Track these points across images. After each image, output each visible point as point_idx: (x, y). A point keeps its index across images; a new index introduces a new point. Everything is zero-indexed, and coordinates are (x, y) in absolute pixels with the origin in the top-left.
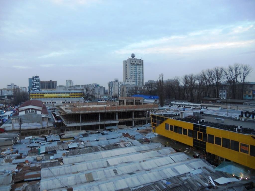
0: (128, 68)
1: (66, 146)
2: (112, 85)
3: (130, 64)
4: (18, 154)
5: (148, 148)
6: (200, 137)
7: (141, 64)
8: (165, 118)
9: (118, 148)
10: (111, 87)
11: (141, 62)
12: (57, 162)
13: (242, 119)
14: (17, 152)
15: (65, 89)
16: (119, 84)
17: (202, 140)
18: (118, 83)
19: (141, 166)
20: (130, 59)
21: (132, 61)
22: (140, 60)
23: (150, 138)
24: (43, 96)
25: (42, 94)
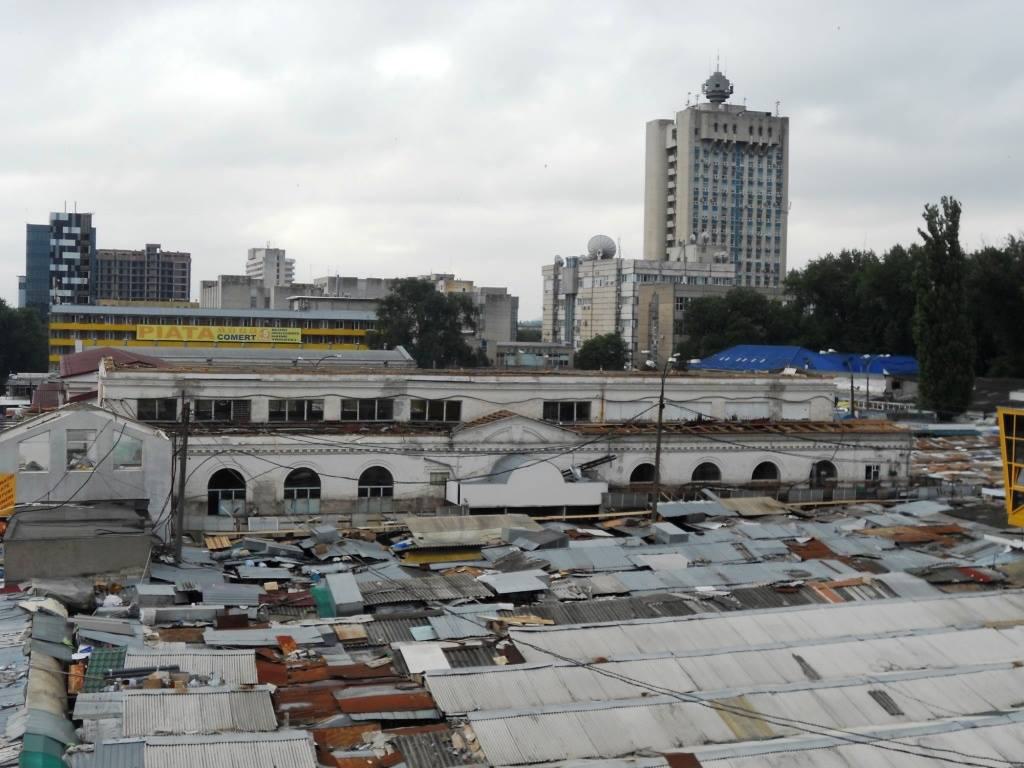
0: (683, 172)
1: (475, 584)
2: (577, 282)
3: (699, 145)
7: (774, 145)
9: (806, 602)
11: (770, 130)
12: (477, 648)
15: (260, 303)
16: (621, 277)
18: (619, 270)
20: (695, 113)
21: (713, 121)
22: (769, 114)
23: (992, 567)
24: (133, 334)
25: (126, 327)
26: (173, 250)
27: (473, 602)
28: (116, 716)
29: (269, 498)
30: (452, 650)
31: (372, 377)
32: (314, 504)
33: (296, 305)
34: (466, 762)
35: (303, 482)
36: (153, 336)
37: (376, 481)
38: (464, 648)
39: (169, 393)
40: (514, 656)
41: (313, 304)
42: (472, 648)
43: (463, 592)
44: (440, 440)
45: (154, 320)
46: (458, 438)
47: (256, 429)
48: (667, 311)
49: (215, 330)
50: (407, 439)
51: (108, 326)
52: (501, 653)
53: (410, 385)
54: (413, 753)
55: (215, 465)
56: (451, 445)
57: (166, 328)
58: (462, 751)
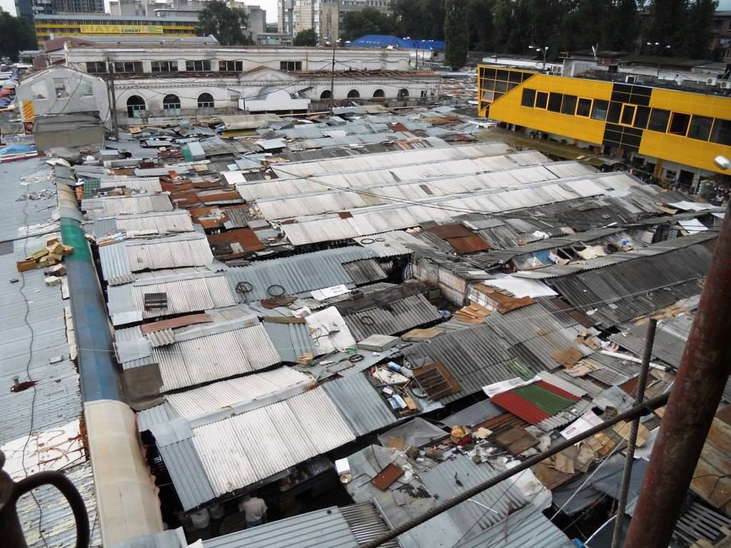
1: (254, 145)
5: (478, 153)
6: (627, 119)
8: (524, 74)
9: (396, 150)
10: (289, 10)
13: (724, 84)
15: (140, 12)
17: (632, 126)
19: (482, 181)
23: (471, 134)
24: (79, 30)
25: (75, 26)
28: (101, 208)
29: (157, 109)
30: (247, 174)
31: (199, 50)
32: (178, 111)
34: (256, 219)
37: (206, 99)
38: (251, 173)
39: (101, 59)
40: (273, 176)
41: (167, 13)
42: (255, 173)
45: (88, 22)
46: (242, 79)
47: (146, 76)
48: (335, 18)
49: (120, 27)
50: (219, 80)
51: (65, 26)
53: (218, 54)
55: (129, 93)
56: (239, 82)
58: (254, 215)
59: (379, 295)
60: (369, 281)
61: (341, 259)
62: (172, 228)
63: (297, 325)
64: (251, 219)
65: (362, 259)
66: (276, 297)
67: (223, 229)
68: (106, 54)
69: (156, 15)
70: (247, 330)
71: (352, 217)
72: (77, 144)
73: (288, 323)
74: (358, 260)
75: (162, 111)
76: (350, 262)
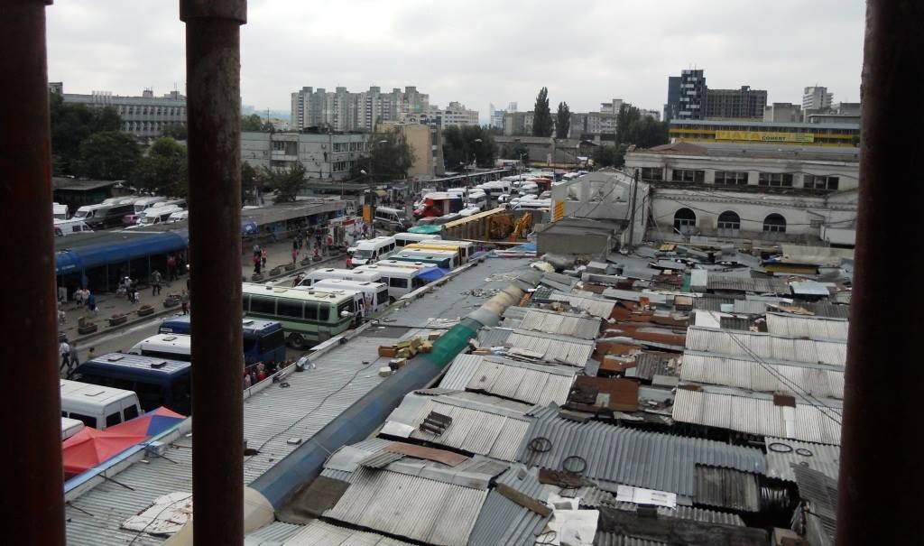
1: (784, 286)
4: (623, 278)
12: (743, 320)
14: (620, 272)
15: (797, 118)
24: (714, 135)
25: (710, 132)
26: (714, 89)
27: (775, 296)
28: (521, 318)
29: (709, 226)
30: (727, 318)
31: (779, 161)
32: (735, 232)
33: (812, 120)
34: (670, 375)
35: (730, 219)
36: (725, 137)
37: (775, 221)
38: (735, 319)
39: (659, 165)
40: (763, 327)
41: (822, 119)
42: (740, 320)
43: (773, 290)
44: (820, 200)
45: (726, 128)
46: (831, 200)
47: (704, 187)
49: (761, 134)
50: (797, 198)
51: (700, 131)
52: (756, 324)
53: (803, 166)
54: (643, 364)
55: (677, 206)
56: (826, 204)
57: (732, 133)
58: (671, 369)
59: (686, 526)
60: (721, 505)
61: (698, 456)
62: (563, 358)
63: (532, 514)
64: (663, 372)
65: (734, 469)
66: (569, 472)
67: (622, 374)
68: (665, 160)
69: (810, 121)
70: (467, 490)
71: (794, 406)
72: (576, 251)
73: (523, 507)
74: (726, 468)
75: (715, 230)
76: (712, 467)
